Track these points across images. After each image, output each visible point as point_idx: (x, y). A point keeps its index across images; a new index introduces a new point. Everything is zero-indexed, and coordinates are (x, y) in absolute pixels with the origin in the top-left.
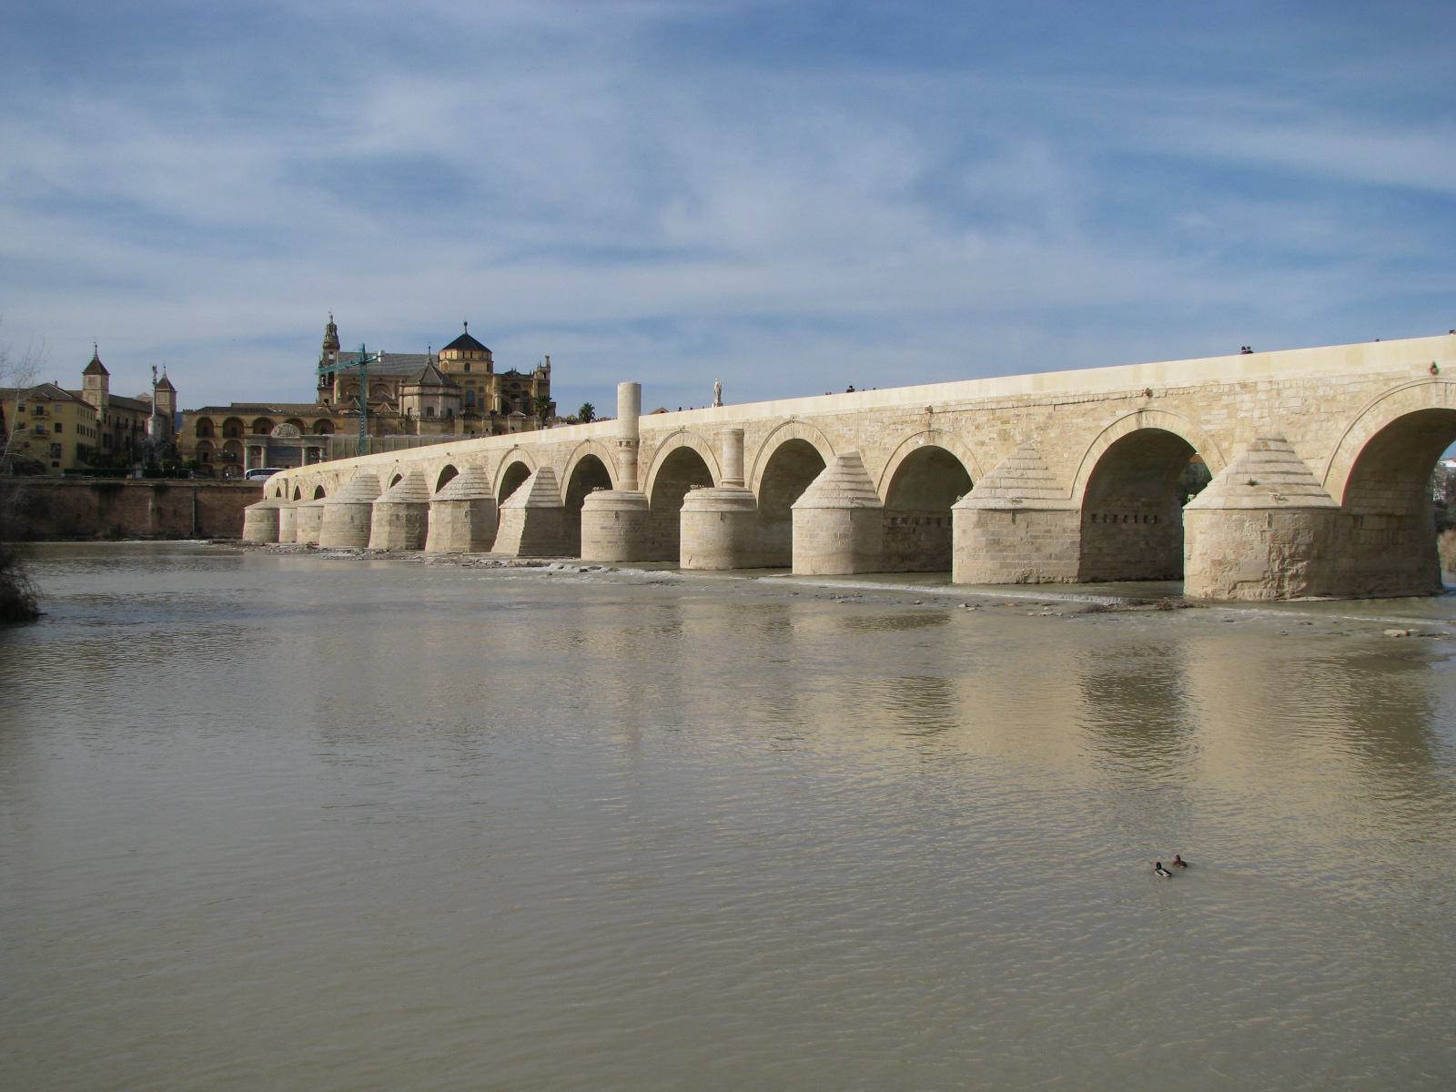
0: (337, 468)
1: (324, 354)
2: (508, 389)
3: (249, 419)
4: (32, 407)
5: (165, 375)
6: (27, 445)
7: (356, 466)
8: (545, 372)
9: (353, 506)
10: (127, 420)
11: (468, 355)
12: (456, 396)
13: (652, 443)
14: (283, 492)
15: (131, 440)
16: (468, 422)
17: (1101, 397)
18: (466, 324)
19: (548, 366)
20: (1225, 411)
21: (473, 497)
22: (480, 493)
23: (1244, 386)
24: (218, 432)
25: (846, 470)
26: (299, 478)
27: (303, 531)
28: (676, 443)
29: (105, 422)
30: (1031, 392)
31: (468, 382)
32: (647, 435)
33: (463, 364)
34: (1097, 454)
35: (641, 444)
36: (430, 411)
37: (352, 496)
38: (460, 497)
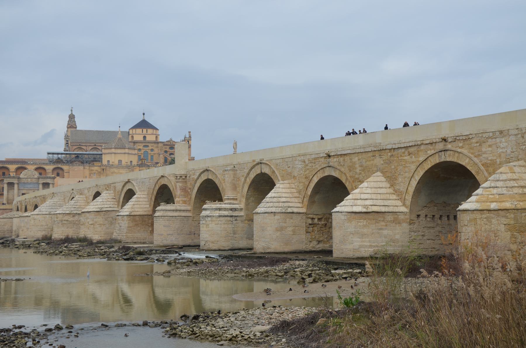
0: (44, 194)
1: (67, 131)
2: (168, 150)
3: (12, 168)
7: (53, 193)
8: (188, 140)
9: (48, 216)
11: (145, 130)
12: (135, 154)
13: (193, 177)
14: (19, 209)
17: (419, 143)
18: (144, 114)
19: (190, 137)
20: (490, 149)
21: (105, 209)
22: (110, 207)
23: (501, 132)
25: (284, 191)
26: (27, 200)
27: (22, 230)
28: (204, 177)
30: (380, 142)
31: (144, 146)
32: (191, 173)
34: (417, 177)
35: (188, 178)
36: (120, 161)
37: (47, 210)
38: (98, 210)
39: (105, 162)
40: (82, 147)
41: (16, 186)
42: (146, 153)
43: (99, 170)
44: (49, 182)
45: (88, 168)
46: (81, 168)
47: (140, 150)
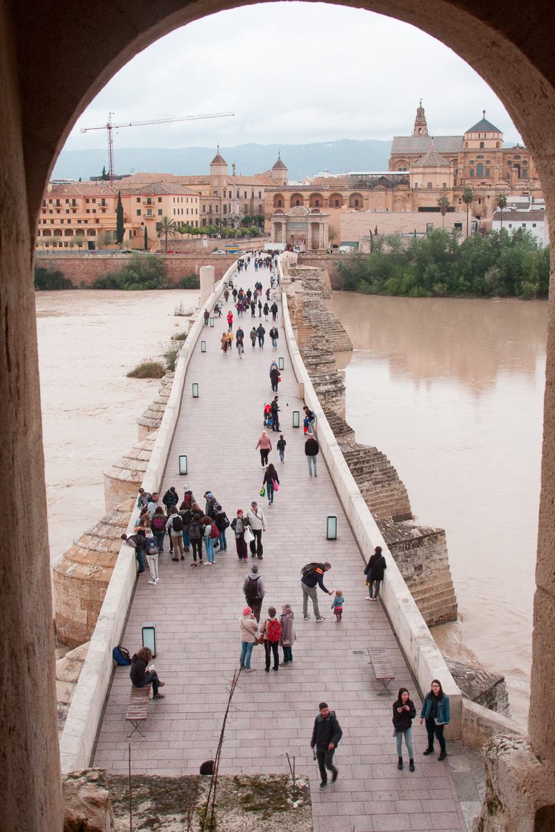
2: (511, 160)
4: (144, 199)
5: (279, 158)
6: (142, 224)
10: (246, 192)
11: (482, 135)
15: (249, 206)
16: (456, 193)
18: (484, 112)
24: (287, 204)
29: (225, 196)
31: (478, 157)
33: (480, 142)
36: (430, 185)
39: (412, 186)
40: (405, 159)
41: (284, 227)
42: (480, 166)
43: (405, 196)
44: (319, 222)
45: (391, 193)
46: (384, 193)
47: (472, 162)
